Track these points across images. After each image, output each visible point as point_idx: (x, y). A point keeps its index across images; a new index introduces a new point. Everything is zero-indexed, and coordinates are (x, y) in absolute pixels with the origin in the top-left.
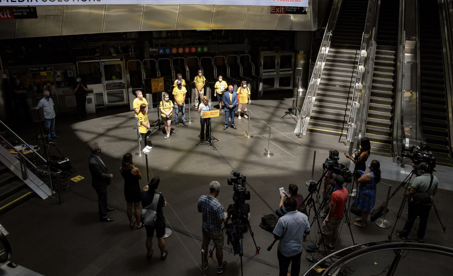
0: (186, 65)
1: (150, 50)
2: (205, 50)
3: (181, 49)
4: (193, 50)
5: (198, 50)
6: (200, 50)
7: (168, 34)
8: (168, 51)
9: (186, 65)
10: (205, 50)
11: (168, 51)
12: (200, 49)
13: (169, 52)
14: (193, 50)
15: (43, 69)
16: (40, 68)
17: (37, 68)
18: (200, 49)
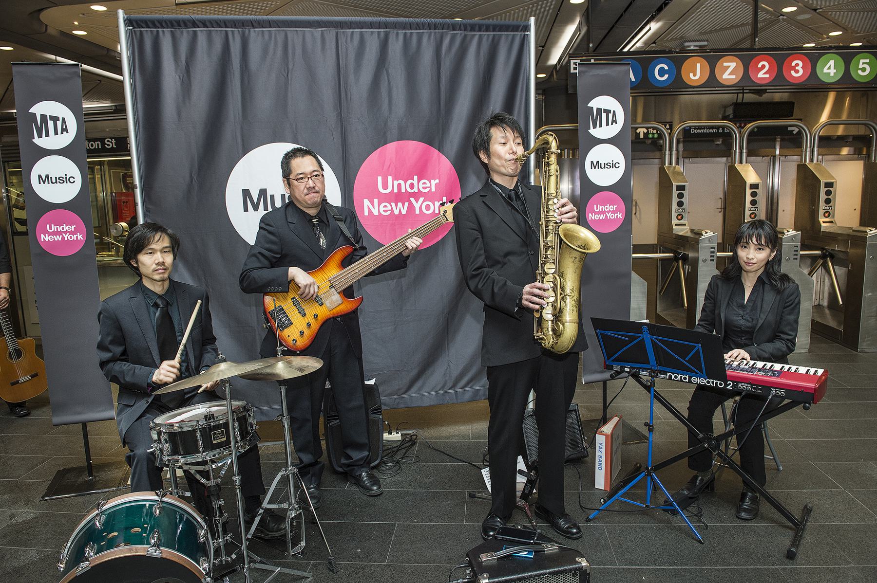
0: (741, 162)
1: (572, 66)
2: (864, 70)
3: (733, 65)
4: (797, 72)
5: (825, 70)
6: (832, 71)
7: (638, 131)
8: (661, 75)
9: (741, 162)
10: (864, 70)
11: (662, 72)
12: (832, 63)
13: (666, 76)
14: (797, 72)
15: (115, 146)
16: (102, 140)
17: (95, 140)
18: (832, 63)
